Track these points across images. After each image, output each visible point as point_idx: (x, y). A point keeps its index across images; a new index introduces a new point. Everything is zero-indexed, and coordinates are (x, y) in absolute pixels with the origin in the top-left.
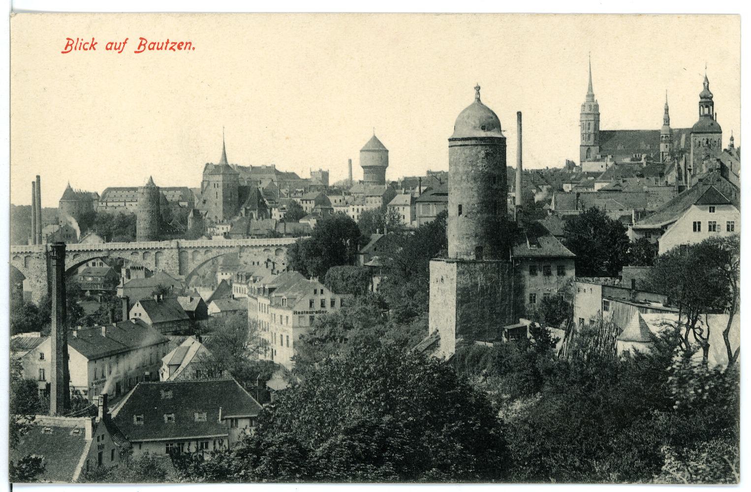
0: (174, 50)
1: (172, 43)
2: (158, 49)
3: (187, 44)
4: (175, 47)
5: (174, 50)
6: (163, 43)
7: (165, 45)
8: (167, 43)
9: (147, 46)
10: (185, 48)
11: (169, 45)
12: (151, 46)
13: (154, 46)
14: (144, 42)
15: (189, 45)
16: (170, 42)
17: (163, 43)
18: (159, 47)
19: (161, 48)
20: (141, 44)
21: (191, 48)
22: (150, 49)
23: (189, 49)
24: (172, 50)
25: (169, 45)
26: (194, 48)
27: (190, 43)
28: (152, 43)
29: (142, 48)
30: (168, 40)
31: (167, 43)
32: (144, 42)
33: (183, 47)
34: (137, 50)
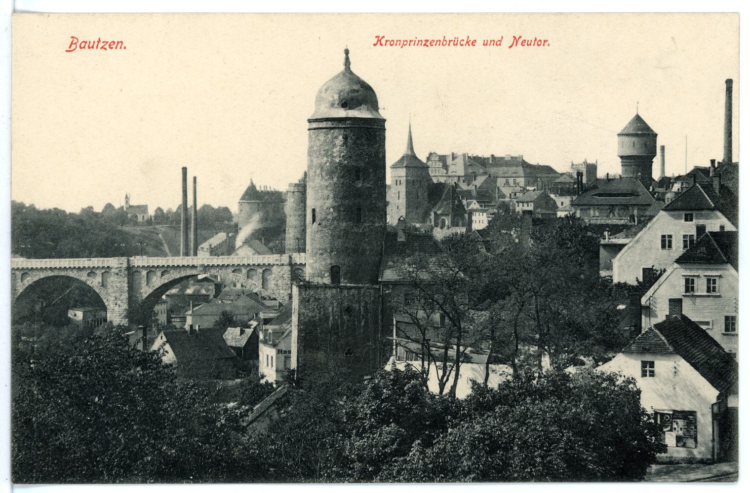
0: (106, 49)
1: (103, 42)
4: (107, 46)
5: (106, 49)
8: (99, 41)
9: (78, 45)
10: (116, 48)
11: (101, 45)
12: (83, 45)
14: (75, 41)
16: (102, 41)
20: (72, 43)
23: (121, 48)
25: (101, 45)
27: (122, 42)
28: (83, 42)
29: (73, 47)
31: (99, 41)
32: (75, 41)
33: (114, 46)
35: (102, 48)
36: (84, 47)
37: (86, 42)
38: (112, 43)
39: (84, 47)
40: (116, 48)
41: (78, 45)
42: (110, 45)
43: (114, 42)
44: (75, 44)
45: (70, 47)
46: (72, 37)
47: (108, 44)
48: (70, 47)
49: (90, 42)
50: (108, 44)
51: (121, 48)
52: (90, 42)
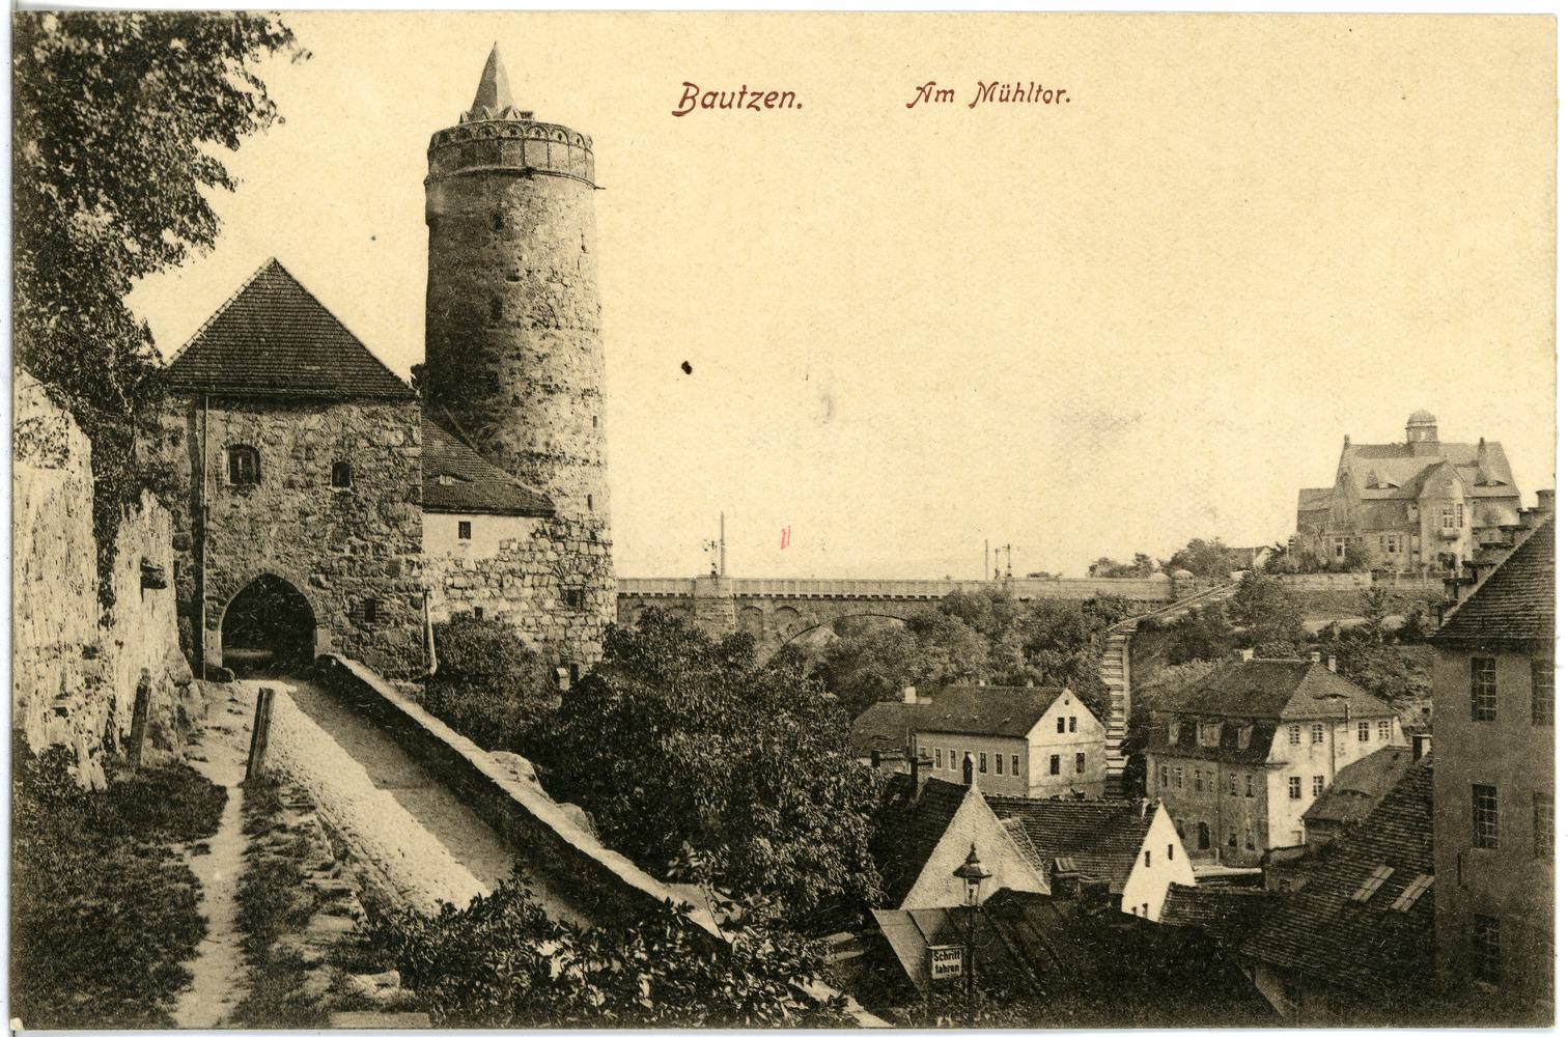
0: (758, 109)
1: (753, 94)
2: (722, 106)
3: (785, 95)
4: (760, 103)
5: (758, 109)
6: (733, 94)
7: (737, 97)
8: (742, 94)
9: (698, 99)
10: (781, 106)
11: (748, 99)
12: (708, 101)
13: (712, 100)
14: (692, 91)
15: (789, 98)
16: (749, 90)
17: (733, 94)
18: (725, 103)
19: (730, 105)
20: (685, 97)
21: (795, 103)
22: (704, 106)
23: (790, 106)
24: (753, 109)
25: (748, 99)
26: (799, 106)
28: (711, 93)
29: (688, 104)
30: (744, 87)
31: (742, 94)
32: (692, 91)
33: (777, 102)
34: (679, 110)
35: (750, 106)
36: (712, 106)
37: (715, 95)
38: (773, 97)
39: (712, 106)
40: (781, 106)
41: (698, 99)
42: (766, 100)
43: (776, 94)
44: (693, 98)
45: (681, 105)
46: (686, 84)
47: (764, 97)
48: (681, 105)
49: (724, 94)
50: (764, 97)
51: (790, 106)
52: (724, 94)
